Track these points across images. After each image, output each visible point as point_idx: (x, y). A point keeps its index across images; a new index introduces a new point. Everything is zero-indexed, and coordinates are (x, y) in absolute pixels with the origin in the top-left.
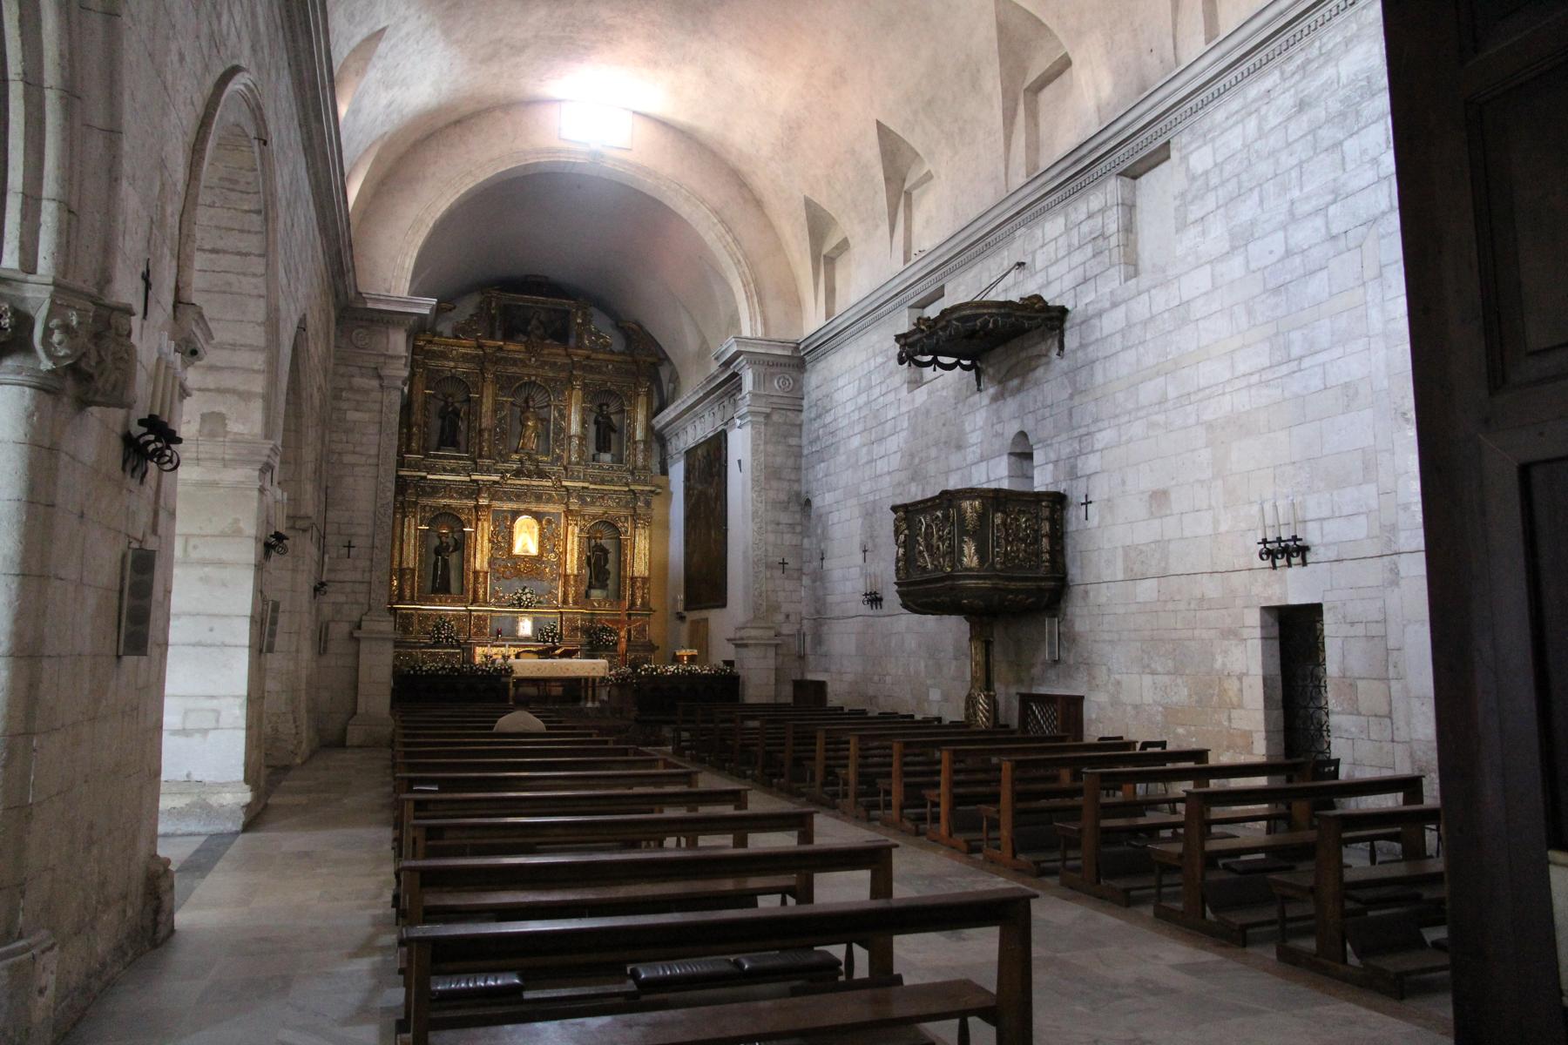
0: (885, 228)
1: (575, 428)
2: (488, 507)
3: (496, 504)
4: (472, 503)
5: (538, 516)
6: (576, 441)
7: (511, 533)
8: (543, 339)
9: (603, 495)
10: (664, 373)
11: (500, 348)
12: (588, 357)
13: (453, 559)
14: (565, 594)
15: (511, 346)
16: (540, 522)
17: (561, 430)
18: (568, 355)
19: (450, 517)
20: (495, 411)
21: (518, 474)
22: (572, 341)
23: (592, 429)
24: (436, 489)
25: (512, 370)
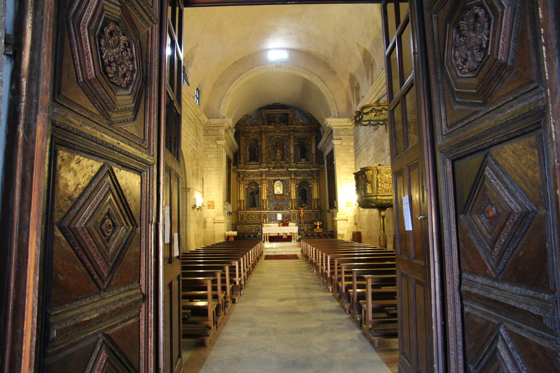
0: (366, 78)
1: (292, 151)
2: (266, 179)
3: (268, 178)
4: (260, 178)
5: (282, 181)
6: (293, 156)
7: (274, 187)
8: (280, 123)
9: (303, 172)
10: (321, 129)
11: (266, 128)
12: (295, 128)
13: (256, 196)
14: (292, 206)
15: (270, 127)
16: (283, 183)
17: (289, 152)
18: (288, 128)
19: (254, 183)
20: (267, 148)
21: (274, 168)
22: (289, 123)
23: (299, 151)
24: (249, 174)
25: (271, 134)
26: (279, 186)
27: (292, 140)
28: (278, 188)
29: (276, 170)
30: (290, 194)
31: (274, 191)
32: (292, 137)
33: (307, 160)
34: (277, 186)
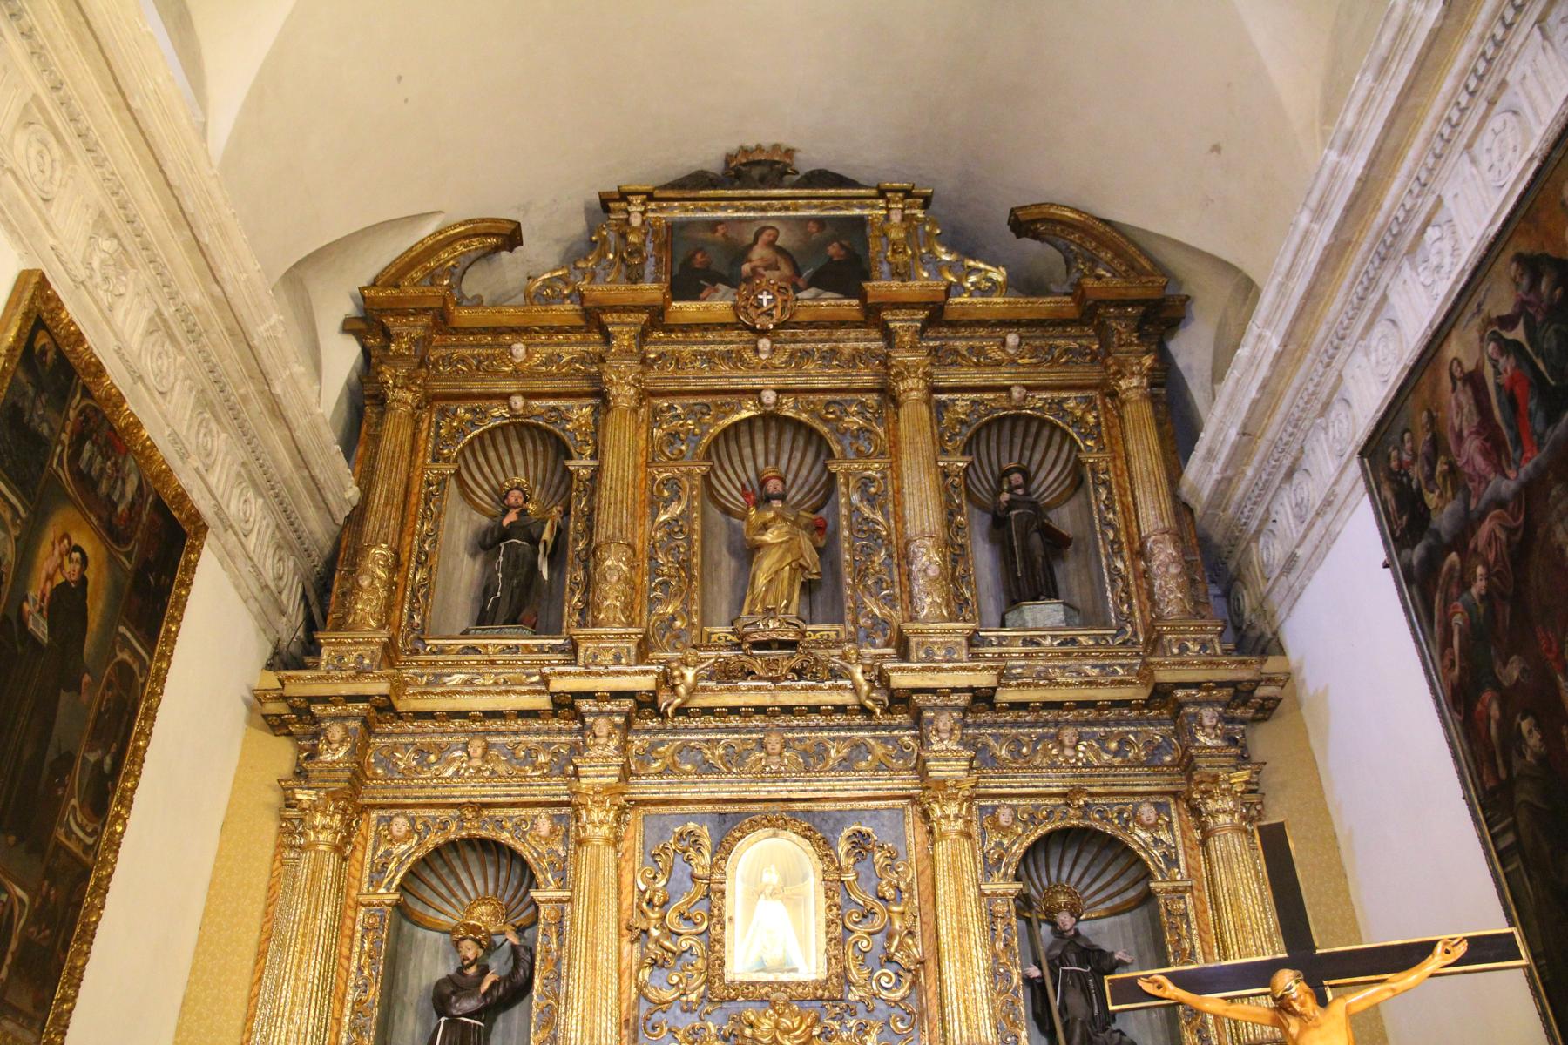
5: (816, 827)
6: (927, 559)
7: (713, 894)
10: (1191, 350)
18: (872, 316)
21: (726, 675)
23: (983, 558)
26: (786, 891)
27: (914, 415)
28: (772, 912)
29: (747, 695)
30: (920, 973)
31: (713, 945)
32: (912, 388)
33: (1085, 615)
34: (758, 893)
